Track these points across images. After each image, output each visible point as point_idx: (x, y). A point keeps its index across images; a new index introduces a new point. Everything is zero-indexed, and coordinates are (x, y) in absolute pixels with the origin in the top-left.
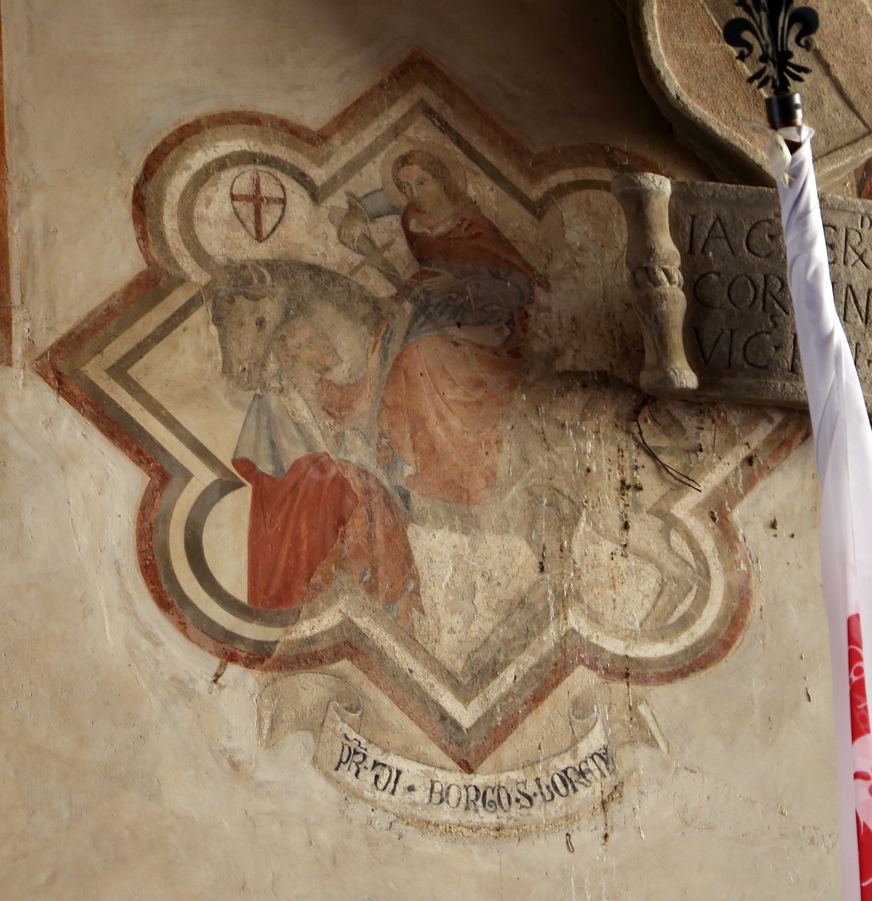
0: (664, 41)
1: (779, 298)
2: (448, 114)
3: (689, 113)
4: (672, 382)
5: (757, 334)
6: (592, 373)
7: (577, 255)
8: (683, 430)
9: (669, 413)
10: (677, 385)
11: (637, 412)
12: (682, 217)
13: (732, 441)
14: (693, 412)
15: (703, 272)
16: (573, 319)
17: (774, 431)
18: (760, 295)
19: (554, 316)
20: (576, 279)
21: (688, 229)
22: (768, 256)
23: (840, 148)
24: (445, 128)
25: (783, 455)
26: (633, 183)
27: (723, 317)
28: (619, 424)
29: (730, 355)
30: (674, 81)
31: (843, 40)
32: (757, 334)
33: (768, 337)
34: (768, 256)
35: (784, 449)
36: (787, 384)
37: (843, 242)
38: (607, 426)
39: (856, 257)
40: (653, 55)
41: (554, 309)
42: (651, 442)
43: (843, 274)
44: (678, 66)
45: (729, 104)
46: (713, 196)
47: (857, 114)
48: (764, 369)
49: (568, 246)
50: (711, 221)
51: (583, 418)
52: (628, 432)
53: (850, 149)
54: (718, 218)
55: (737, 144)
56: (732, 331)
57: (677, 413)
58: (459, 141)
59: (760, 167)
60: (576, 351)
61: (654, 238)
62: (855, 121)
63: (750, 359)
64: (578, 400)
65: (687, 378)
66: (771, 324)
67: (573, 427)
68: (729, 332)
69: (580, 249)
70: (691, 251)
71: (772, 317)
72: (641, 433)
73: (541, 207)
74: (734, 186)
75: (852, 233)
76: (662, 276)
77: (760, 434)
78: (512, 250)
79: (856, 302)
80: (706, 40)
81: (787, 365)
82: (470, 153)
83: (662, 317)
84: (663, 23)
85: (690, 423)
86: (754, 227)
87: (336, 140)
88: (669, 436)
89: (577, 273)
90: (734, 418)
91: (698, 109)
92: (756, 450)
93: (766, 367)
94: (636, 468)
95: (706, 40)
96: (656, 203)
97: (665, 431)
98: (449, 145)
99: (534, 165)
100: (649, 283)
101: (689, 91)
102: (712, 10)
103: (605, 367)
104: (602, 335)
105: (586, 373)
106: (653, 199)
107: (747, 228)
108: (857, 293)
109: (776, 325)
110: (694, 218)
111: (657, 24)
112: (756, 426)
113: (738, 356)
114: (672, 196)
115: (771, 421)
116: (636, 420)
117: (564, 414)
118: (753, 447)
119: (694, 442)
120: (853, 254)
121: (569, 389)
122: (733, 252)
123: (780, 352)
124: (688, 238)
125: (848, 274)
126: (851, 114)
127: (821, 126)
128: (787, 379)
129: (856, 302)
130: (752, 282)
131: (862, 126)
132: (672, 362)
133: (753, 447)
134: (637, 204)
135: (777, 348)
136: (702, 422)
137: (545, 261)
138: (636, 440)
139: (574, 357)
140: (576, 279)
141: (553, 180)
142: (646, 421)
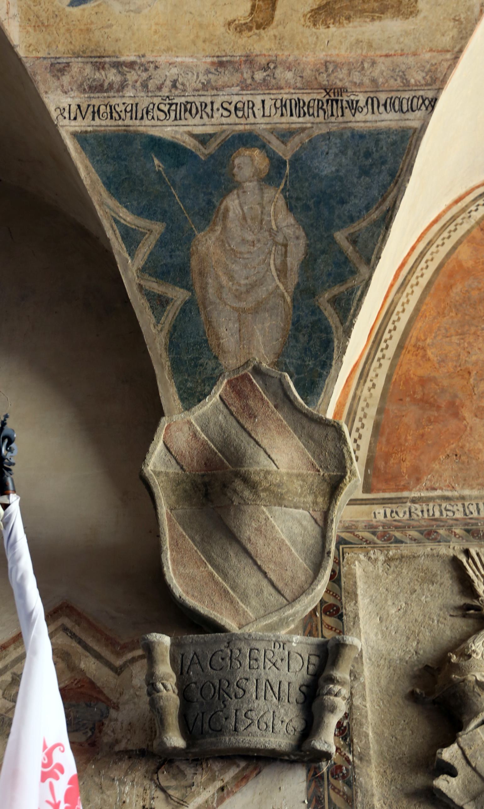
0: (173, 570)
1: (227, 691)
2: (77, 630)
3: (187, 604)
4: (165, 744)
5: (215, 713)
6: (136, 750)
7: (137, 691)
8: (184, 775)
9: (178, 767)
10: (168, 745)
11: (159, 768)
12: (176, 656)
13: (213, 779)
14: (192, 765)
15: (188, 683)
16: (130, 724)
17: (240, 772)
18: (217, 691)
19: (119, 723)
20: (135, 703)
21: (179, 662)
22: (221, 669)
23: (272, 613)
24: (73, 636)
25: (243, 784)
26: (144, 639)
27: (198, 706)
28: (147, 776)
29: (202, 726)
30: (178, 588)
31: (274, 559)
32: (215, 713)
33: (221, 713)
34: (221, 669)
35: (245, 780)
36: (232, 738)
37: (263, 657)
38: (139, 777)
39: (271, 665)
40: (167, 578)
41: (120, 720)
42: (164, 784)
43: (263, 674)
44: (181, 581)
45: (210, 598)
46: (192, 642)
47: (283, 595)
48: (220, 731)
49: (133, 687)
50: (192, 655)
51: (126, 774)
52: (152, 779)
53: (277, 613)
54: (195, 653)
55: (213, 616)
56: (203, 713)
57: (183, 767)
58: (80, 642)
59: (224, 626)
60: (129, 740)
61: (157, 667)
62: (281, 599)
63: (212, 727)
64: (124, 765)
65: (175, 740)
66: (223, 706)
67: (119, 780)
68: (201, 715)
69: (140, 688)
70: (182, 673)
71: (223, 702)
72: (158, 779)
73: (121, 669)
74: (203, 635)
75: (268, 652)
76: (160, 686)
77: (230, 774)
78: (100, 692)
79: (272, 689)
80: (198, 567)
81: (232, 727)
82: (86, 647)
83: (162, 709)
84: (173, 561)
85: (189, 771)
86: (213, 655)
87: (11, 648)
88: (176, 779)
89: (136, 700)
90: (216, 766)
91: (191, 601)
92: (227, 783)
93: (221, 730)
94: (153, 798)
95: (198, 567)
96: (158, 649)
97: (174, 777)
98: (74, 644)
99: (121, 649)
100: (154, 692)
101: (187, 593)
102: (202, 553)
103: (144, 747)
104: (146, 730)
105: (132, 751)
106: (156, 646)
107: (210, 656)
108: (272, 684)
109: (225, 706)
110: (183, 655)
111: (170, 562)
112: (229, 770)
113: (206, 726)
114: (171, 645)
115: (238, 766)
116: (157, 773)
117: (115, 774)
118: (225, 781)
119: (190, 782)
120: (269, 663)
121: (120, 760)
122: (203, 671)
123: (228, 720)
124: (180, 667)
125: (266, 674)
126: (280, 596)
127: (262, 603)
128: (233, 735)
129: (272, 689)
130: (213, 685)
131: (285, 601)
132: (167, 733)
133: (225, 781)
134: (149, 650)
135: (226, 719)
136: (197, 770)
137: (118, 696)
138: (155, 783)
139: (127, 743)
140: (135, 703)
141: (130, 656)
142: (163, 773)
